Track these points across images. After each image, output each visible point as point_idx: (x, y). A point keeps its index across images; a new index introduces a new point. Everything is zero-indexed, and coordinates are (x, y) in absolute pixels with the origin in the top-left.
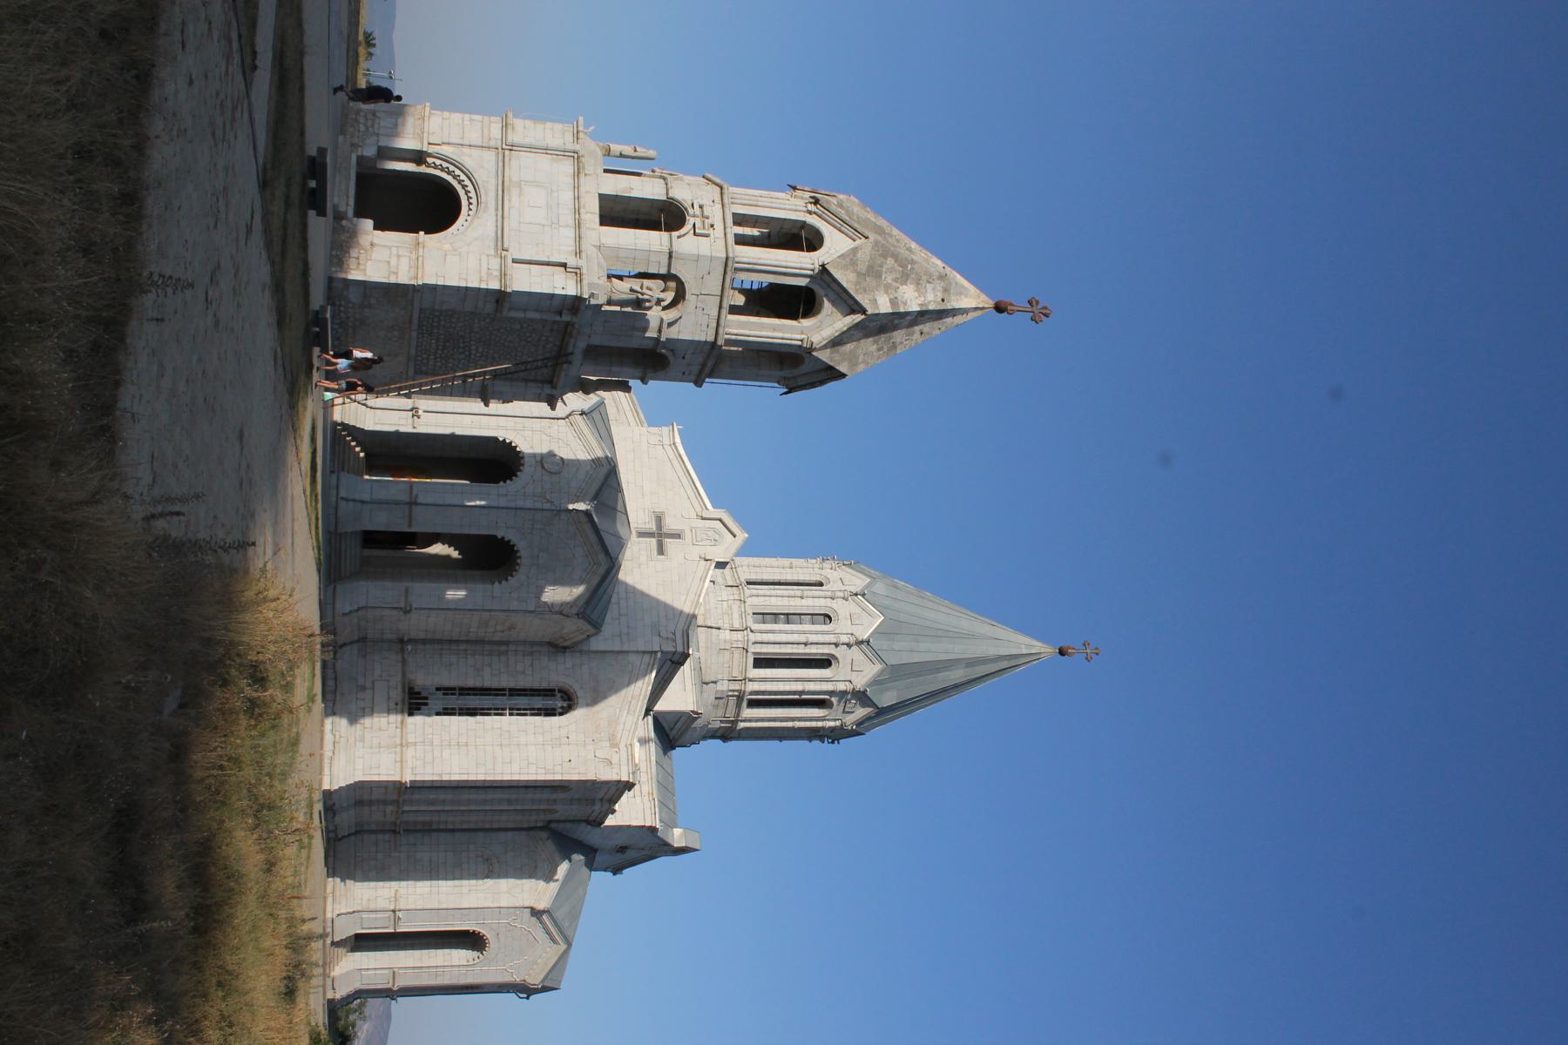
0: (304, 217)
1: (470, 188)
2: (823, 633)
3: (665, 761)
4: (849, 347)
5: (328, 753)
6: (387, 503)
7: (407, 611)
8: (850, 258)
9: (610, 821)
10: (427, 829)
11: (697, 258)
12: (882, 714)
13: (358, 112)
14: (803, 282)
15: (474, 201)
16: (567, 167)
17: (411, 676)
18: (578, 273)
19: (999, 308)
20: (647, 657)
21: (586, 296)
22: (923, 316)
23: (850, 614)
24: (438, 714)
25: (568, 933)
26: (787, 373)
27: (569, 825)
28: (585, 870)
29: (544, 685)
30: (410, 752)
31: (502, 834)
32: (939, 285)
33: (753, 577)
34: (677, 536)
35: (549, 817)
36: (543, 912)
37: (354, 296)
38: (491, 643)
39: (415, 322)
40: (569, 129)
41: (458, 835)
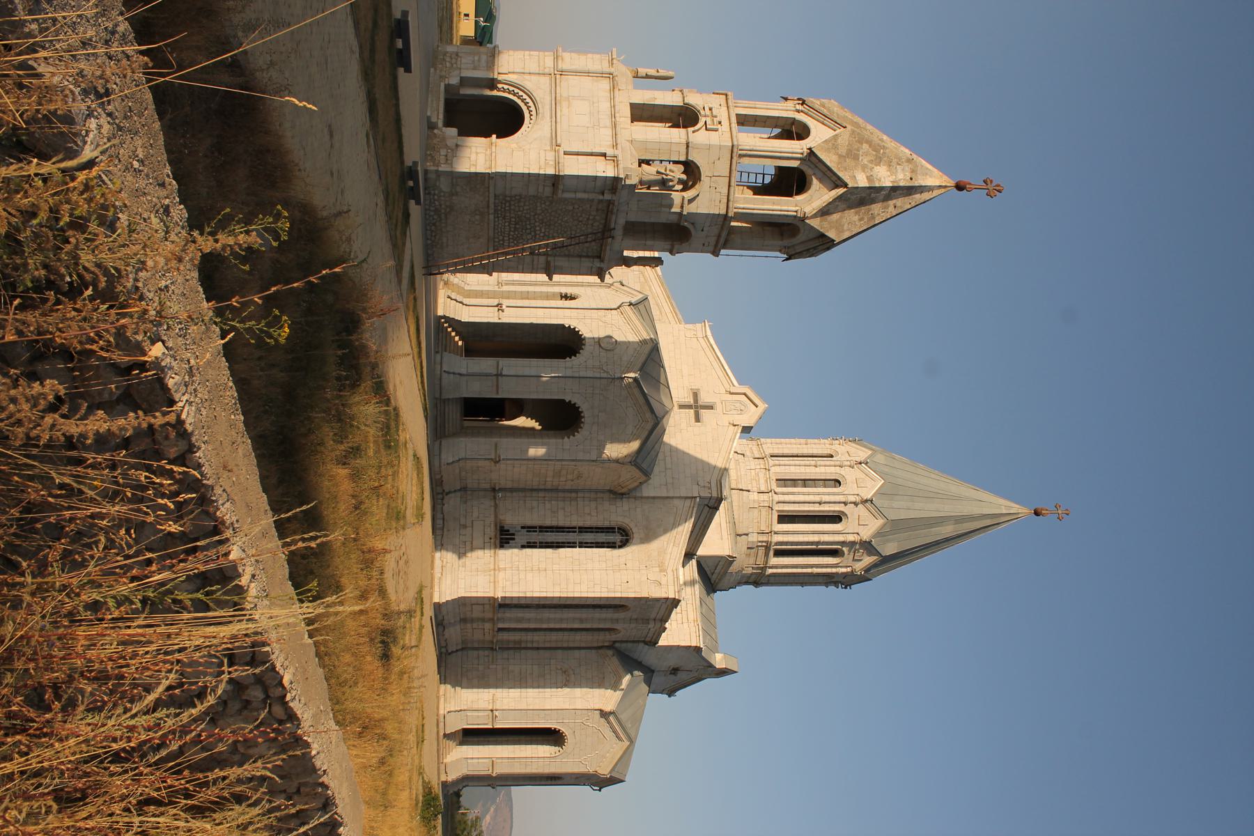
0: (395, 78)
1: (531, 104)
2: (834, 494)
3: (708, 599)
4: (835, 217)
5: (437, 575)
6: (480, 375)
7: (496, 462)
8: (832, 143)
9: (664, 641)
10: (518, 647)
11: (709, 147)
12: (886, 562)
13: (445, 54)
14: (795, 164)
15: (534, 113)
16: (605, 84)
17: (502, 517)
18: (615, 159)
19: (960, 187)
21: (622, 176)
22: (895, 191)
23: (858, 481)
24: (523, 547)
25: (632, 735)
26: (786, 242)
27: (630, 645)
28: (645, 688)
29: (607, 524)
30: (501, 575)
31: (577, 652)
32: (908, 167)
33: (776, 452)
35: (614, 637)
36: (611, 713)
37: (444, 185)
38: (564, 491)
39: (492, 206)
40: (606, 58)
41: (541, 652)
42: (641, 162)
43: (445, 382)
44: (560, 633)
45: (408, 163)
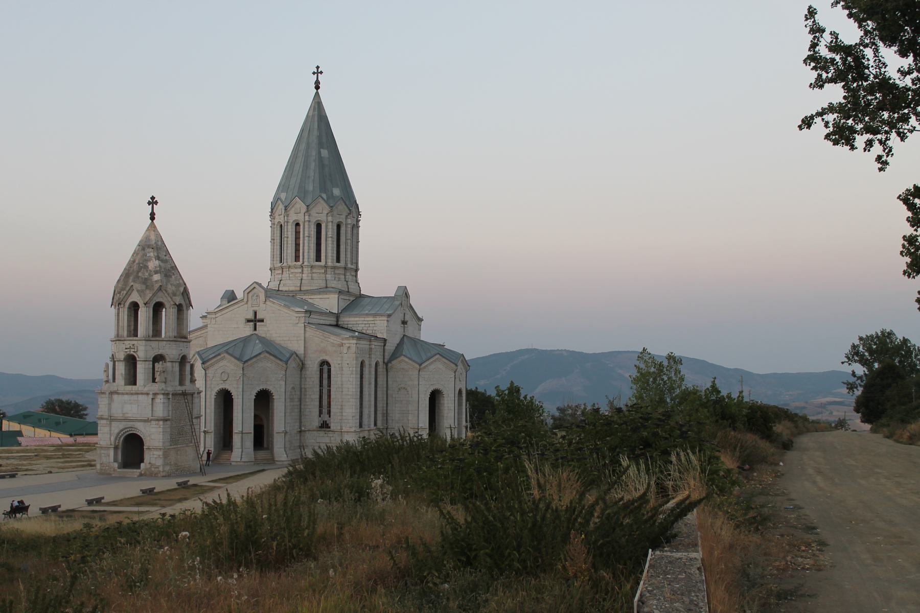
7: (286, 433)
10: (386, 415)
11: (146, 351)
16: (115, 397)
18: (155, 394)
20: (307, 329)
26: (185, 308)
27: (386, 354)
29: (318, 373)
30: (344, 429)
31: (390, 383)
32: (148, 250)
33: (279, 259)
35: (381, 363)
37: (167, 468)
42: (154, 380)
44: (378, 393)
45: (176, 487)
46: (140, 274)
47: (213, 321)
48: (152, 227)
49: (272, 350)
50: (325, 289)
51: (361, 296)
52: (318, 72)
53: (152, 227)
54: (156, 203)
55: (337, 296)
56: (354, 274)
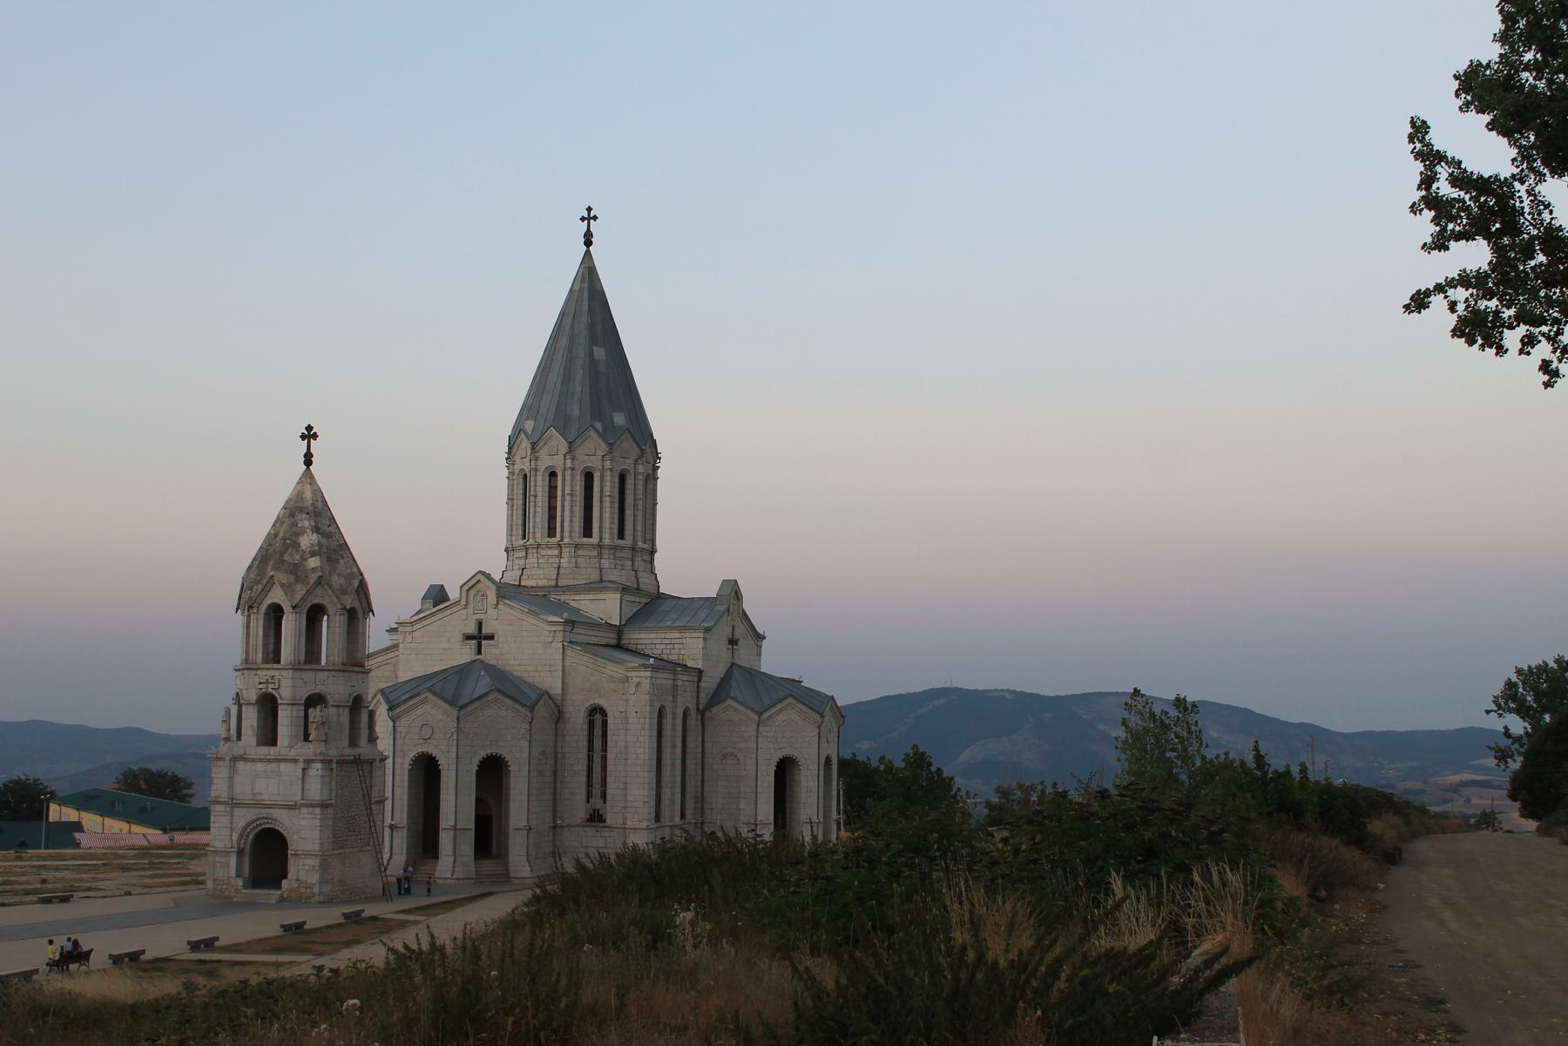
8: (288, 589)
10: (701, 800)
11: (294, 687)
16: (241, 765)
18: (308, 762)
26: (360, 615)
27: (702, 695)
29: (586, 727)
30: (630, 824)
34: (480, 624)
35: (693, 711)
37: (327, 888)
42: (306, 738)
43: (461, 876)
45: (341, 920)
46: (286, 557)
47: (409, 638)
48: (308, 477)
49: (507, 686)
50: (599, 585)
51: (661, 597)
52: (589, 218)
53: (308, 477)
54: (315, 436)
55: (618, 596)
56: (647, 558)
